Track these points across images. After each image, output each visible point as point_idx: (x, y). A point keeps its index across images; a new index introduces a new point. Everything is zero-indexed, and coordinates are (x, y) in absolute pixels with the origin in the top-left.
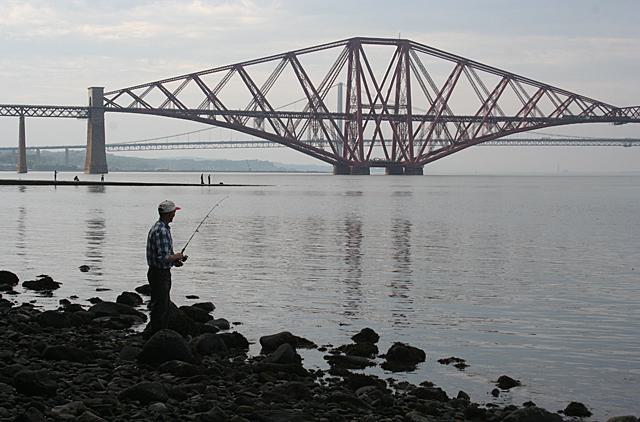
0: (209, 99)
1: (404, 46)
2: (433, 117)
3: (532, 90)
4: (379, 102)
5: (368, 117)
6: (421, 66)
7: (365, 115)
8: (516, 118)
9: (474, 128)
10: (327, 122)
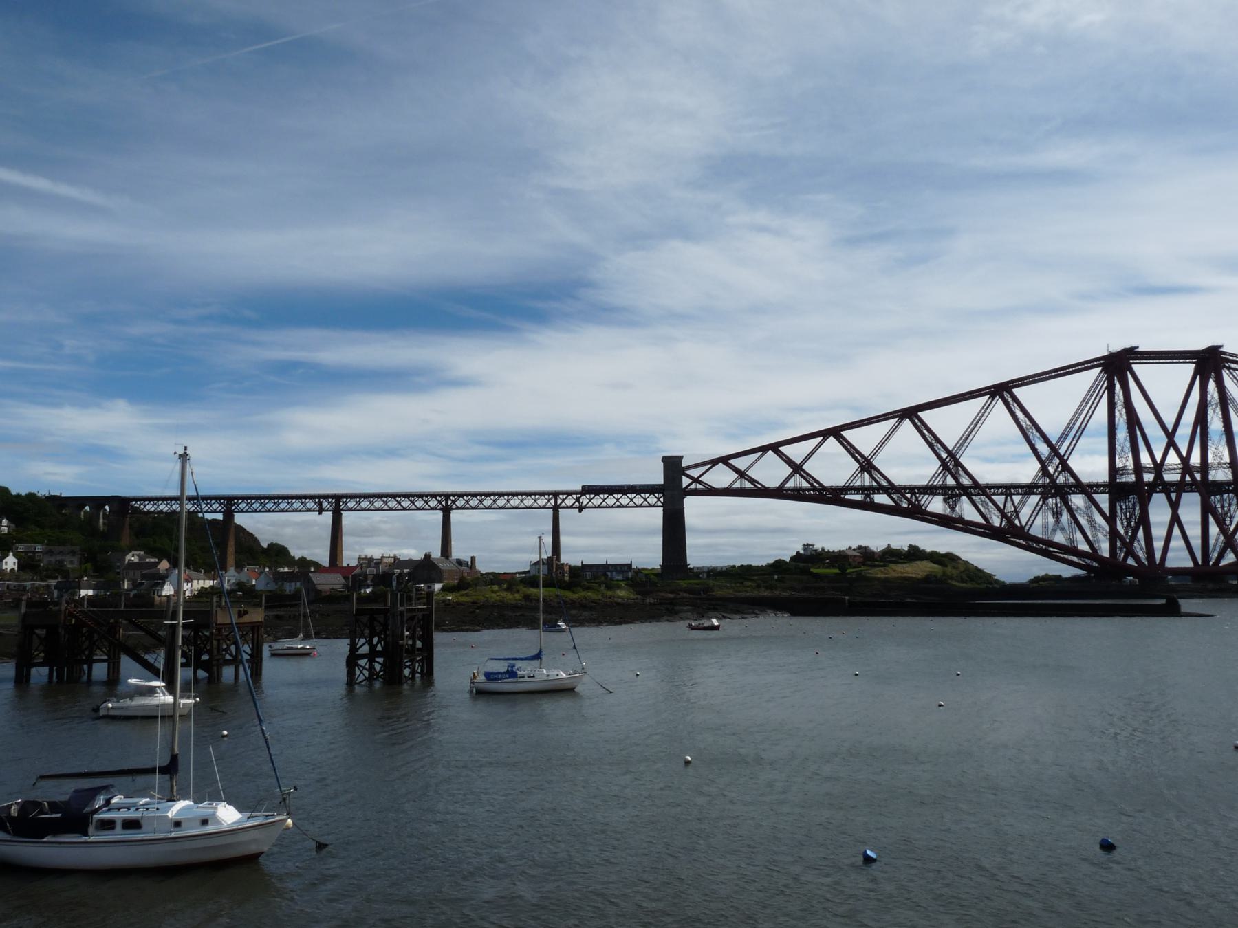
4: (1173, 458)
7: (1148, 484)
10: (1078, 500)
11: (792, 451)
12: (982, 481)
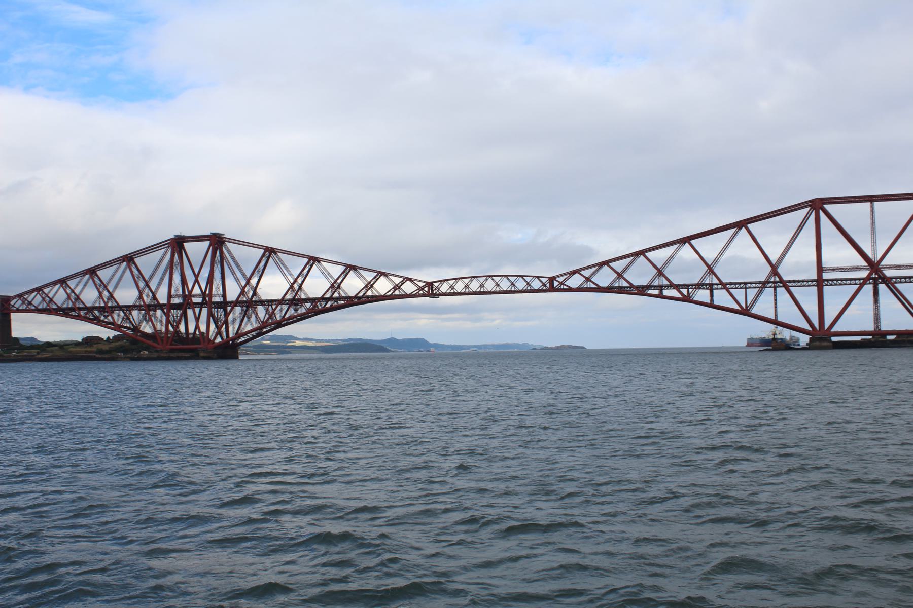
0: (69, 296)
1: (217, 241)
2: (240, 302)
3: (336, 271)
6: (233, 258)
8: (323, 298)
9: (281, 310)
11: (46, 291)
12: (121, 304)
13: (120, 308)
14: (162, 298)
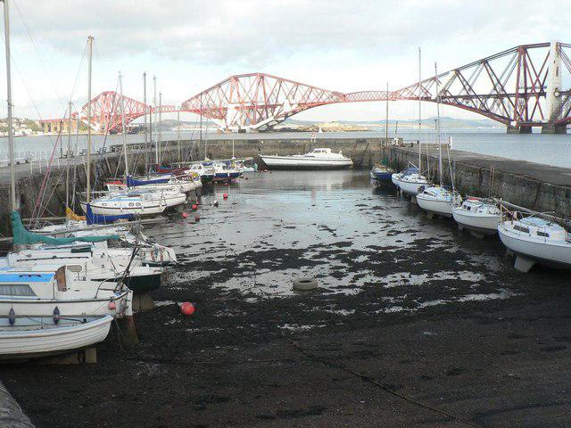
4: (538, 85)
5: (531, 94)
10: (506, 99)
13: (477, 97)
14: (511, 89)
